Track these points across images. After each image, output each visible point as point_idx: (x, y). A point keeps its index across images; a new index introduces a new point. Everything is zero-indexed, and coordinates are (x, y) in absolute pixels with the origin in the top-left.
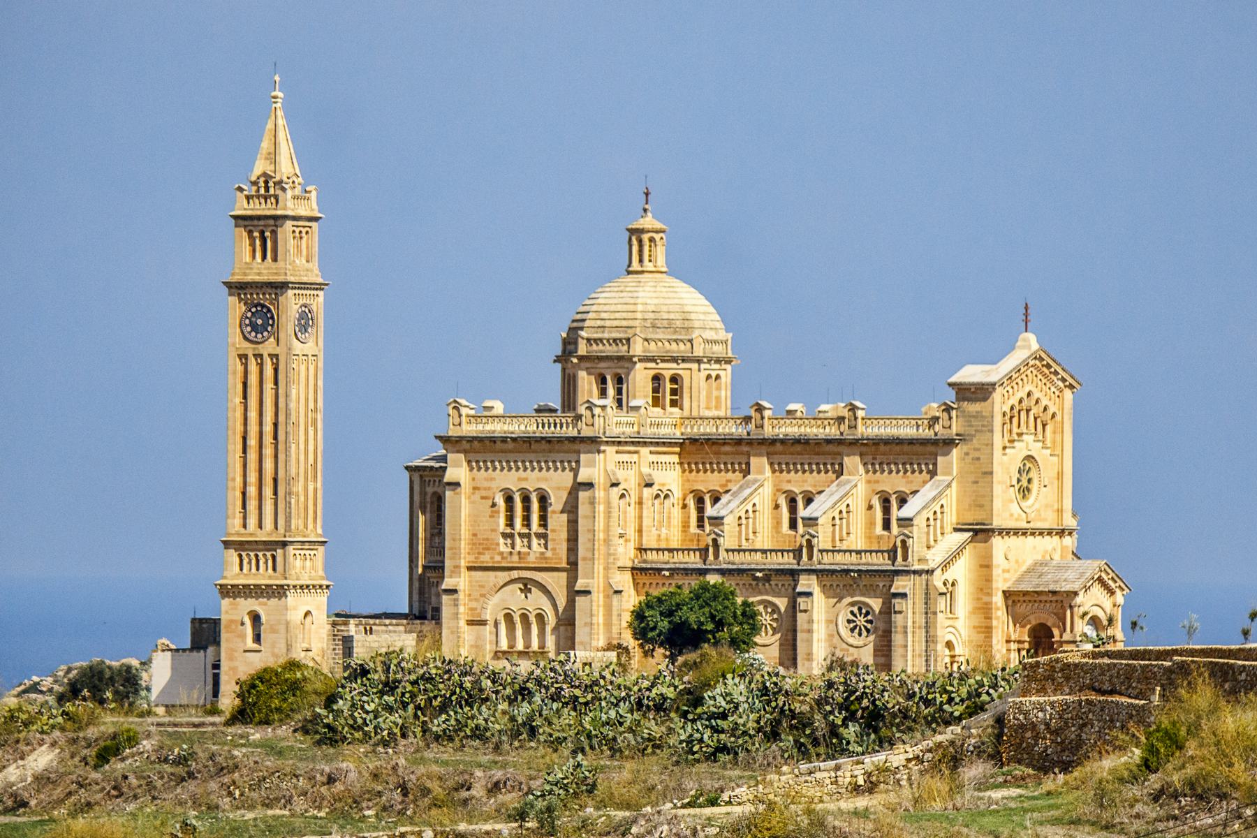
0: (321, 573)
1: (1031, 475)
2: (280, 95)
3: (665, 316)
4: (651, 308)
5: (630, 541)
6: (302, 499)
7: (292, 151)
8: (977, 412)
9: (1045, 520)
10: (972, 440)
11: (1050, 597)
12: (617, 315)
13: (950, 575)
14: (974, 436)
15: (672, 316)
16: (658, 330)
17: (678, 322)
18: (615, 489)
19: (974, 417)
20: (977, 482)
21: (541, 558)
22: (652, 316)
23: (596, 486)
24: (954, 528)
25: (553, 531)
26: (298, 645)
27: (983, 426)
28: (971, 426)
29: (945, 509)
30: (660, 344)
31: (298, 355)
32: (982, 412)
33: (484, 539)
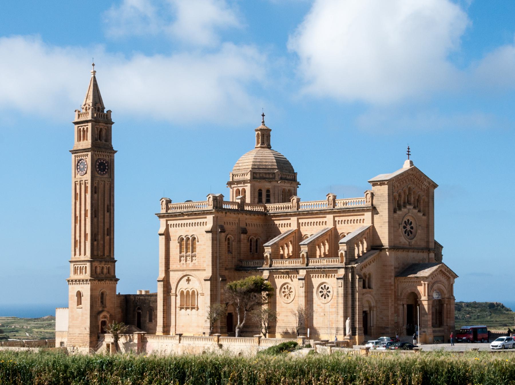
1: (412, 225)
3: (264, 164)
4: (258, 160)
6: (102, 242)
8: (381, 194)
10: (379, 207)
12: (245, 164)
14: (380, 205)
15: (267, 164)
17: (269, 166)
19: (380, 196)
20: (381, 227)
21: (194, 266)
22: (258, 163)
25: (198, 253)
27: (384, 200)
28: (378, 201)
32: (383, 194)
33: (174, 258)
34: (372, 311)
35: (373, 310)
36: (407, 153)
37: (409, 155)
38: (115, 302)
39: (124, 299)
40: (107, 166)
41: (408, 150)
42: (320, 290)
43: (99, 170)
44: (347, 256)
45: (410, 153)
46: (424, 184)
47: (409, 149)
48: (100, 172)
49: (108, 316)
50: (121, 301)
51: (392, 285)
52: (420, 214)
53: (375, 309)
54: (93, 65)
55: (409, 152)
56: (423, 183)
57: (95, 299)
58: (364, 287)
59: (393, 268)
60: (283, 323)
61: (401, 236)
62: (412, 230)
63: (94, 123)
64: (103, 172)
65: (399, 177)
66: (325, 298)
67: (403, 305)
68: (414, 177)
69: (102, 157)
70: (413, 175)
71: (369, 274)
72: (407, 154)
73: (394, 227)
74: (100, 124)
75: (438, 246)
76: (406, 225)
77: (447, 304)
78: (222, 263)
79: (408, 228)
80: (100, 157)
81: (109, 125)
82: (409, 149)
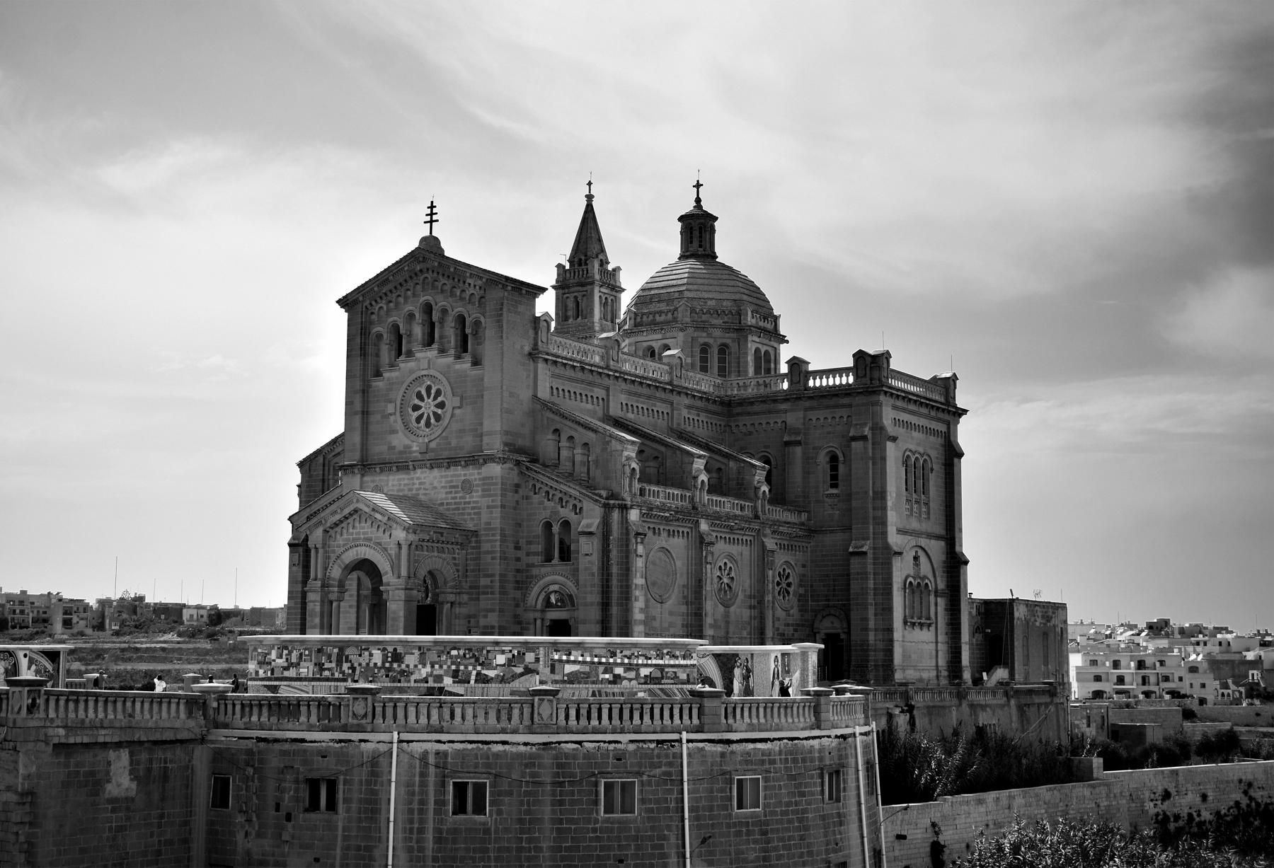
36: (428, 218)
41: (429, 211)
45: (435, 217)
46: (470, 284)
47: (432, 207)
52: (465, 365)
54: (590, 184)
56: (464, 282)
63: (561, 291)
65: (376, 289)
68: (435, 275)
70: (428, 269)
72: (425, 222)
74: (572, 290)
79: (428, 406)
81: (589, 287)
82: (432, 207)
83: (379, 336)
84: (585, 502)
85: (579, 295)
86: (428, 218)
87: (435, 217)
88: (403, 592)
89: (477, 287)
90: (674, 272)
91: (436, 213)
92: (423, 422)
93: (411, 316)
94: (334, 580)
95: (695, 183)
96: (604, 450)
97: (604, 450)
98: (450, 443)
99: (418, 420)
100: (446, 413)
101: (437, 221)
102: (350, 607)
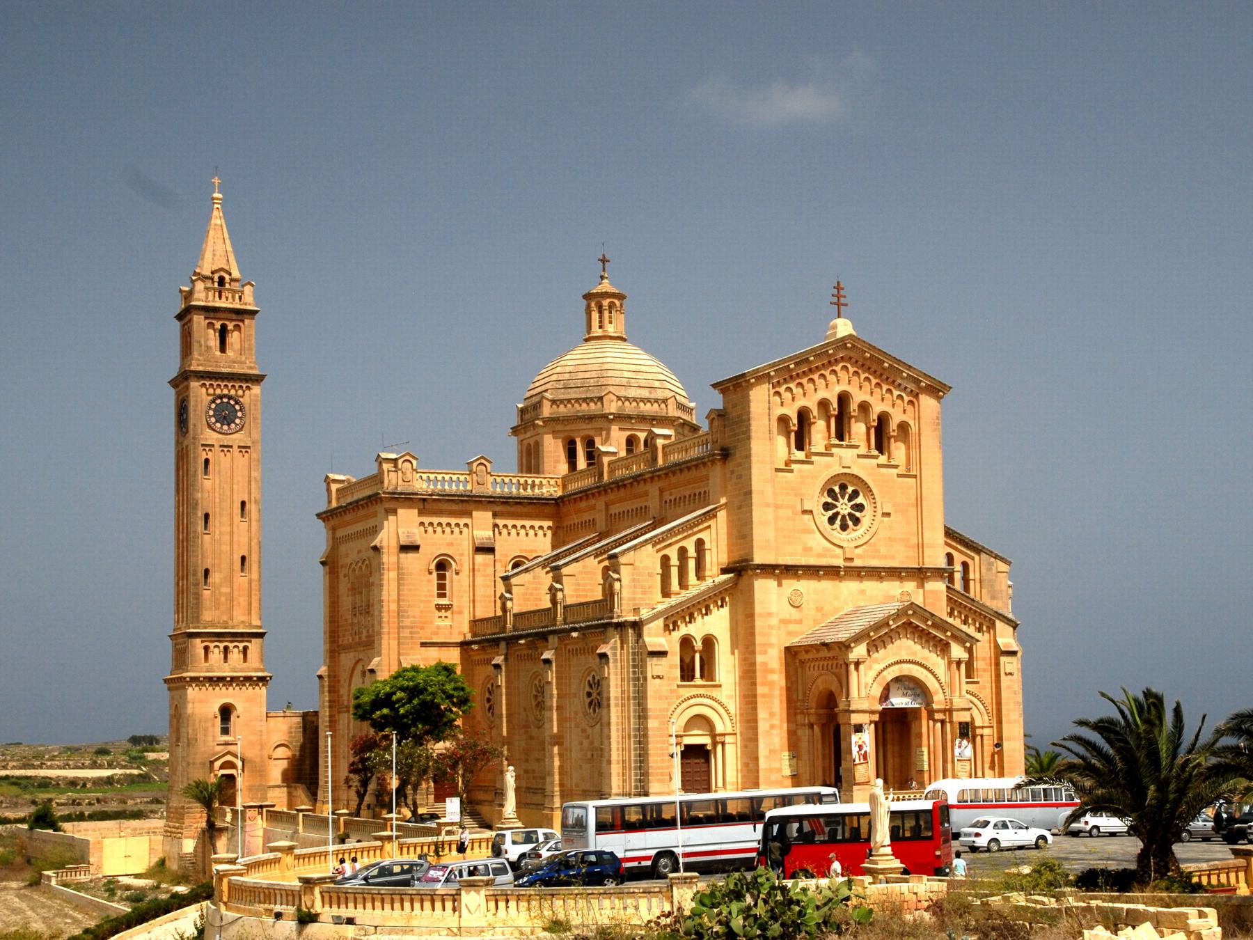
0: (257, 664)
2: (220, 196)
3: (581, 375)
5: (460, 612)
7: (229, 248)
9: (892, 557)
11: (824, 653)
13: (697, 629)
15: (588, 375)
16: (569, 390)
17: (592, 380)
18: (411, 556)
22: (567, 376)
23: (385, 550)
24: (722, 569)
26: (210, 739)
29: (707, 546)
30: (569, 406)
31: (213, 446)
34: (719, 748)
35: (723, 744)
36: (835, 300)
37: (839, 304)
38: (261, 731)
39: (298, 723)
40: (241, 410)
41: (835, 292)
42: (588, 689)
43: (217, 421)
44: (624, 591)
45: (842, 300)
47: (838, 287)
48: (218, 425)
49: (239, 764)
50: (291, 728)
51: (772, 671)
53: (728, 739)
55: (839, 296)
56: (894, 382)
57: (203, 723)
58: (687, 673)
59: (774, 621)
60: (534, 778)
61: (810, 532)
62: (858, 514)
64: (229, 425)
66: (594, 711)
67: (811, 726)
69: (225, 392)
71: (709, 642)
73: (776, 506)
75: (992, 560)
76: (837, 500)
77: (943, 722)
78: (412, 628)
79: (844, 507)
80: (218, 392)
82: (838, 287)
83: (783, 420)
84: (997, 622)
85: (230, 326)
86: (835, 300)
87: (842, 300)
88: (853, 707)
89: (909, 390)
90: (589, 351)
91: (844, 297)
92: (838, 522)
93: (824, 404)
94: (874, 698)
95: (607, 258)
96: (989, 570)
97: (989, 570)
98: (879, 551)
99: (832, 520)
100: (866, 517)
101: (846, 305)
102: (772, 727)
